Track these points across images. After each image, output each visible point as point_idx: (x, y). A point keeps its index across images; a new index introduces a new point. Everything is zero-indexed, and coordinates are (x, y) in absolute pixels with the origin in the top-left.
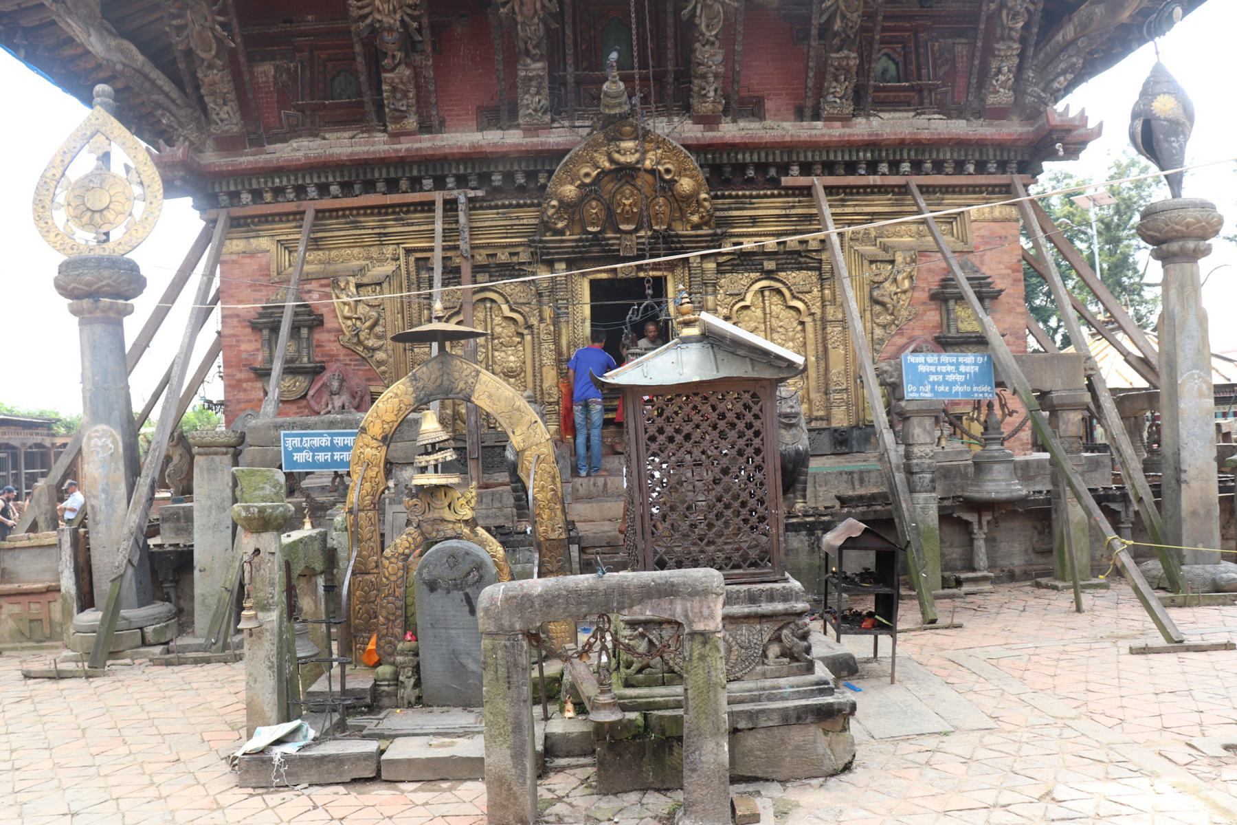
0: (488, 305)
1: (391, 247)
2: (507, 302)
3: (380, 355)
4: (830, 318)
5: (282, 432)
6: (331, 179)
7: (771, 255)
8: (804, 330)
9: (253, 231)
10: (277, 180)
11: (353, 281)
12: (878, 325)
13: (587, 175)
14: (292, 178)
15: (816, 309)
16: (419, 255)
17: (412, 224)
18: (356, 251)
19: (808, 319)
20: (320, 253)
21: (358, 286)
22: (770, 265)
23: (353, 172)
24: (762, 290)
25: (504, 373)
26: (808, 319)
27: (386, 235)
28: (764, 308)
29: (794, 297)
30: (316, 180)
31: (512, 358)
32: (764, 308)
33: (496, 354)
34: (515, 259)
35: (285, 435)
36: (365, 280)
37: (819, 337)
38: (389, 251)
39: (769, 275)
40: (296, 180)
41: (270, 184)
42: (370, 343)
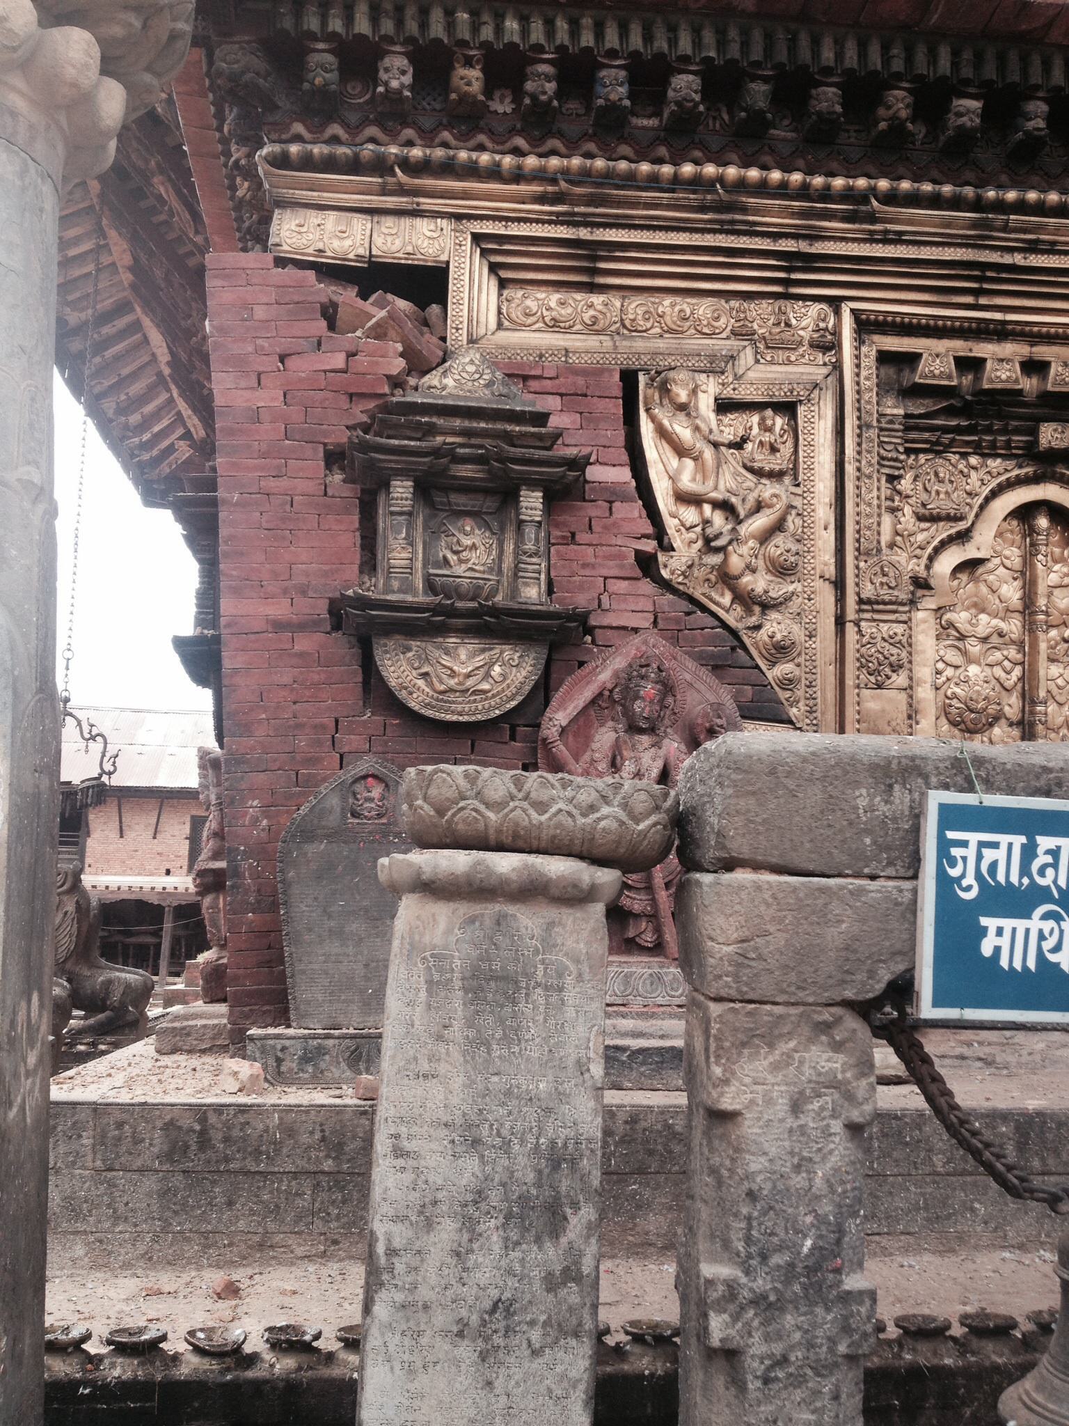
0: (1043, 522)
1: (815, 309)
3: (776, 626)
5: (936, 798)
6: (685, 44)
9: (402, 191)
10: (512, 25)
11: (710, 389)
14: (562, 25)
16: (893, 343)
17: (898, 239)
18: (704, 308)
20: (597, 299)
21: (724, 406)
23: (757, 35)
27: (809, 261)
30: (636, 41)
35: (952, 817)
36: (747, 393)
38: (807, 318)
40: (575, 33)
41: (487, 33)
42: (759, 583)
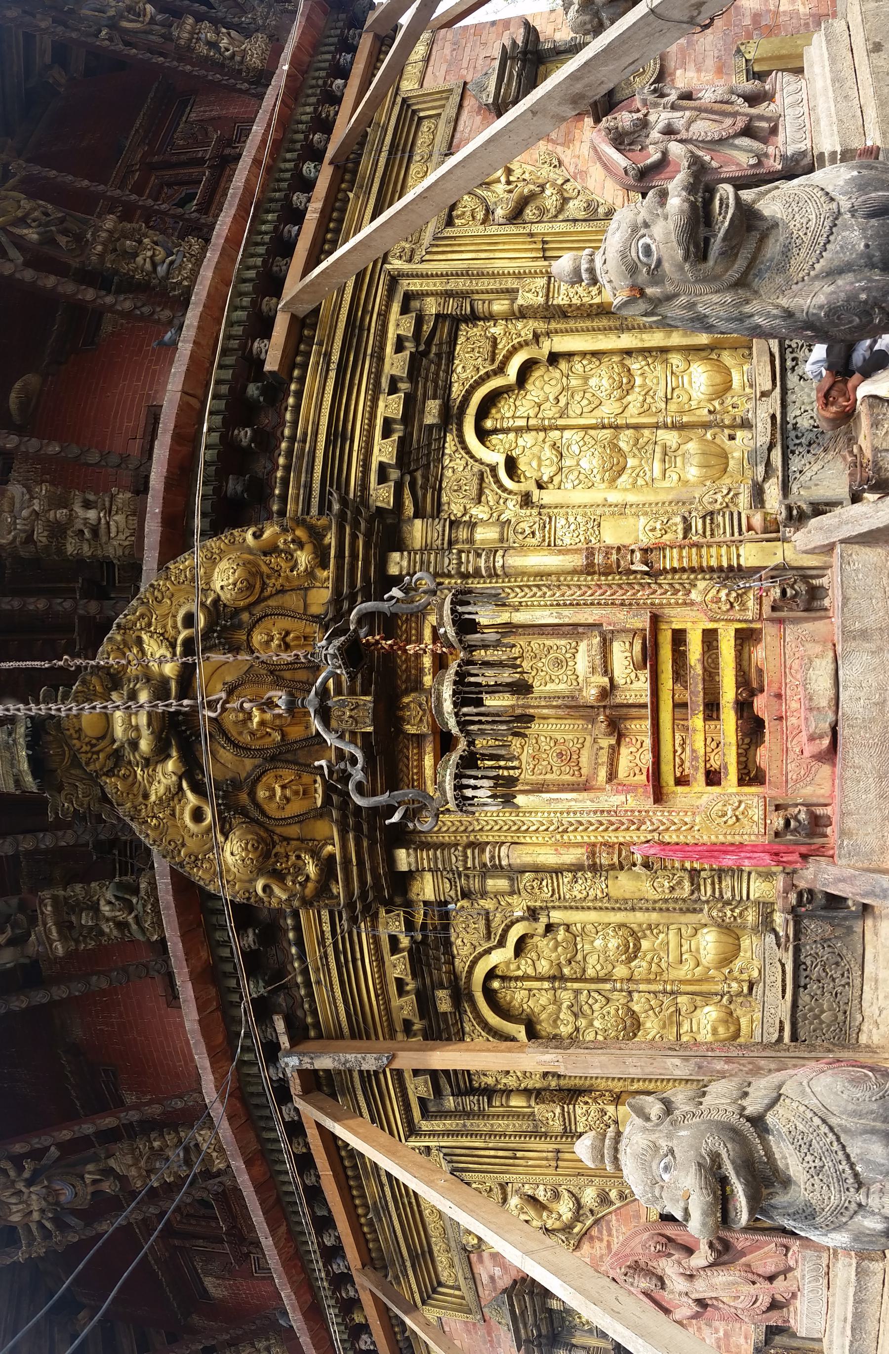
2: (488, 951)
4: (541, 300)
7: (412, 407)
8: (569, 356)
12: (561, 210)
13: (197, 815)
15: (525, 329)
19: (546, 347)
22: (432, 411)
24: (482, 435)
25: (630, 960)
26: (546, 347)
28: (519, 430)
29: (501, 370)
31: (598, 943)
32: (519, 430)
33: (590, 972)
34: (405, 942)
37: (580, 324)
39: (451, 417)
